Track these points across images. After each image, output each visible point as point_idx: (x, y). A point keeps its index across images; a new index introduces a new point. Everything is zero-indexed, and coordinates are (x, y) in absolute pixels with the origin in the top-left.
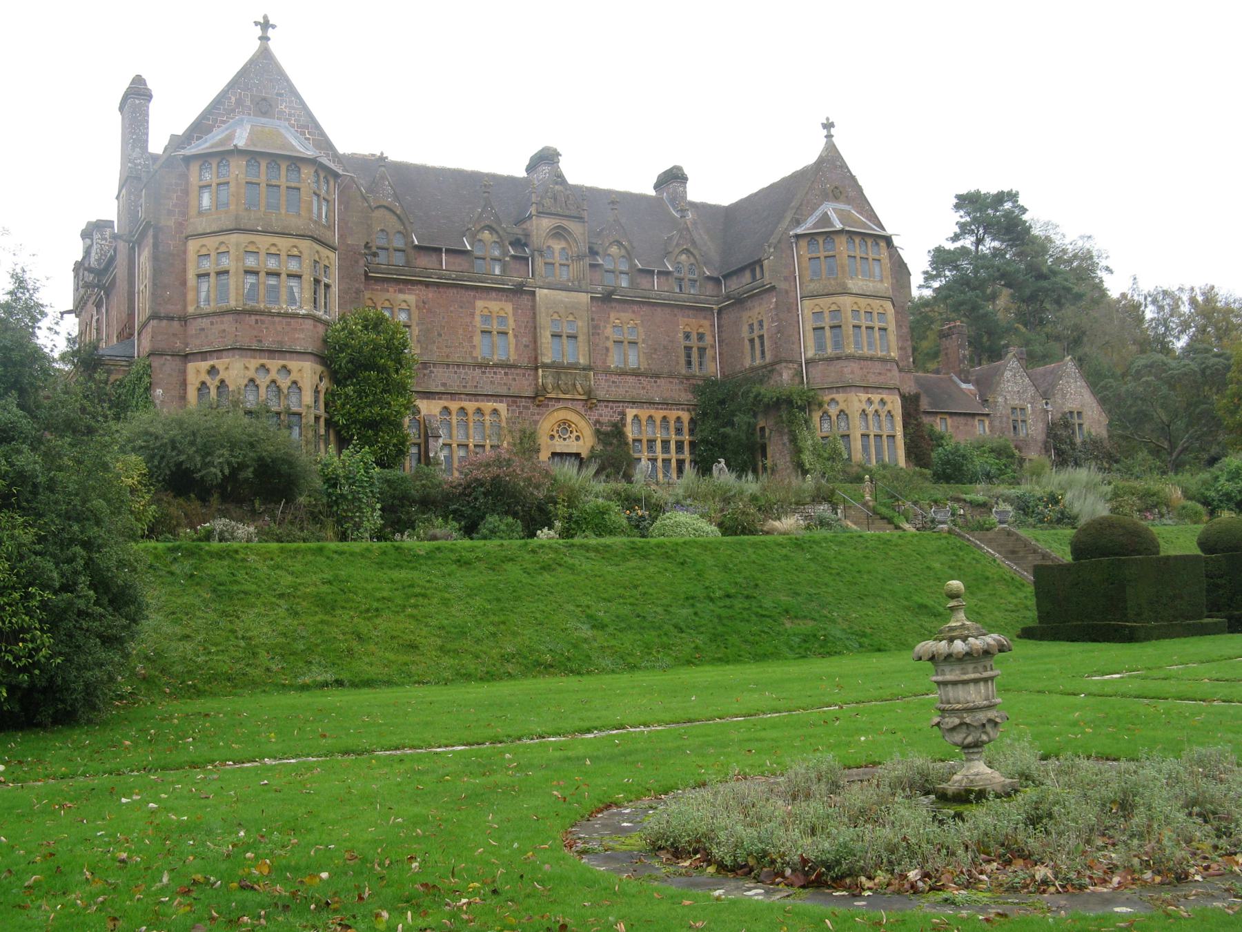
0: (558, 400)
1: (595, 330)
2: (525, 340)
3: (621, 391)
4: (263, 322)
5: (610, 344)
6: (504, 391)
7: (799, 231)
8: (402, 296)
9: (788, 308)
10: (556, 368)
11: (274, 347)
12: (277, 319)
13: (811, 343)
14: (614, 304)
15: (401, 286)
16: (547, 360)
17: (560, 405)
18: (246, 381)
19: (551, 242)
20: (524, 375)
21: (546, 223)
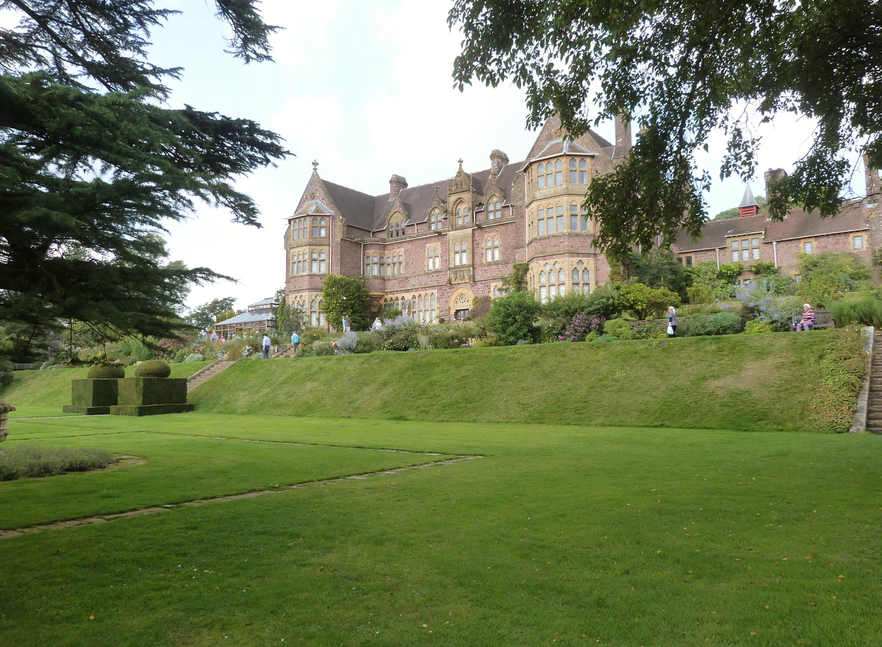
2: (445, 258)
3: (489, 274)
5: (483, 251)
16: (452, 266)
21: (453, 198)
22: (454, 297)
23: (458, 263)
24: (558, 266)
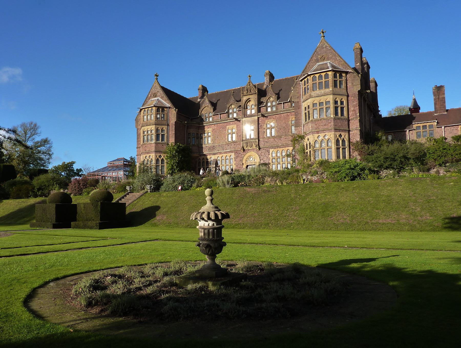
0: (249, 150)
5: (265, 130)
22: (245, 158)
24: (326, 138)
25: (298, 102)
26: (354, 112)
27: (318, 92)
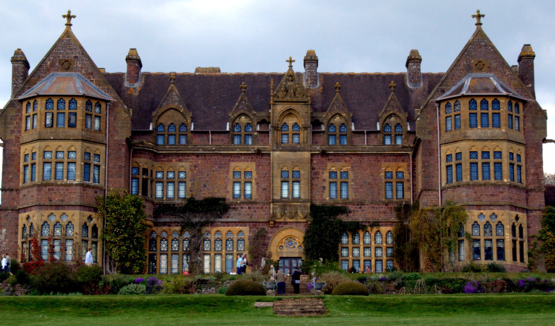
0: (286, 223)
1: (314, 174)
2: (264, 185)
4: (53, 190)
6: (247, 219)
7: (439, 99)
8: (181, 164)
9: (431, 153)
10: (283, 202)
11: (58, 203)
12: (60, 188)
13: (444, 176)
14: (330, 157)
15: (181, 158)
16: (277, 197)
17: (287, 226)
18: (42, 223)
19: (285, 120)
20: (262, 208)
21: (280, 108)
23: (285, 194)
25: (430, 142)
26: (535, 177)
27: (479, 132)
